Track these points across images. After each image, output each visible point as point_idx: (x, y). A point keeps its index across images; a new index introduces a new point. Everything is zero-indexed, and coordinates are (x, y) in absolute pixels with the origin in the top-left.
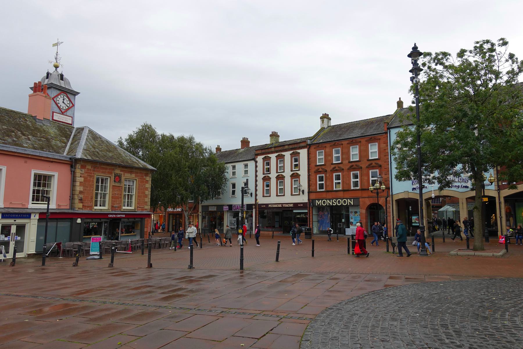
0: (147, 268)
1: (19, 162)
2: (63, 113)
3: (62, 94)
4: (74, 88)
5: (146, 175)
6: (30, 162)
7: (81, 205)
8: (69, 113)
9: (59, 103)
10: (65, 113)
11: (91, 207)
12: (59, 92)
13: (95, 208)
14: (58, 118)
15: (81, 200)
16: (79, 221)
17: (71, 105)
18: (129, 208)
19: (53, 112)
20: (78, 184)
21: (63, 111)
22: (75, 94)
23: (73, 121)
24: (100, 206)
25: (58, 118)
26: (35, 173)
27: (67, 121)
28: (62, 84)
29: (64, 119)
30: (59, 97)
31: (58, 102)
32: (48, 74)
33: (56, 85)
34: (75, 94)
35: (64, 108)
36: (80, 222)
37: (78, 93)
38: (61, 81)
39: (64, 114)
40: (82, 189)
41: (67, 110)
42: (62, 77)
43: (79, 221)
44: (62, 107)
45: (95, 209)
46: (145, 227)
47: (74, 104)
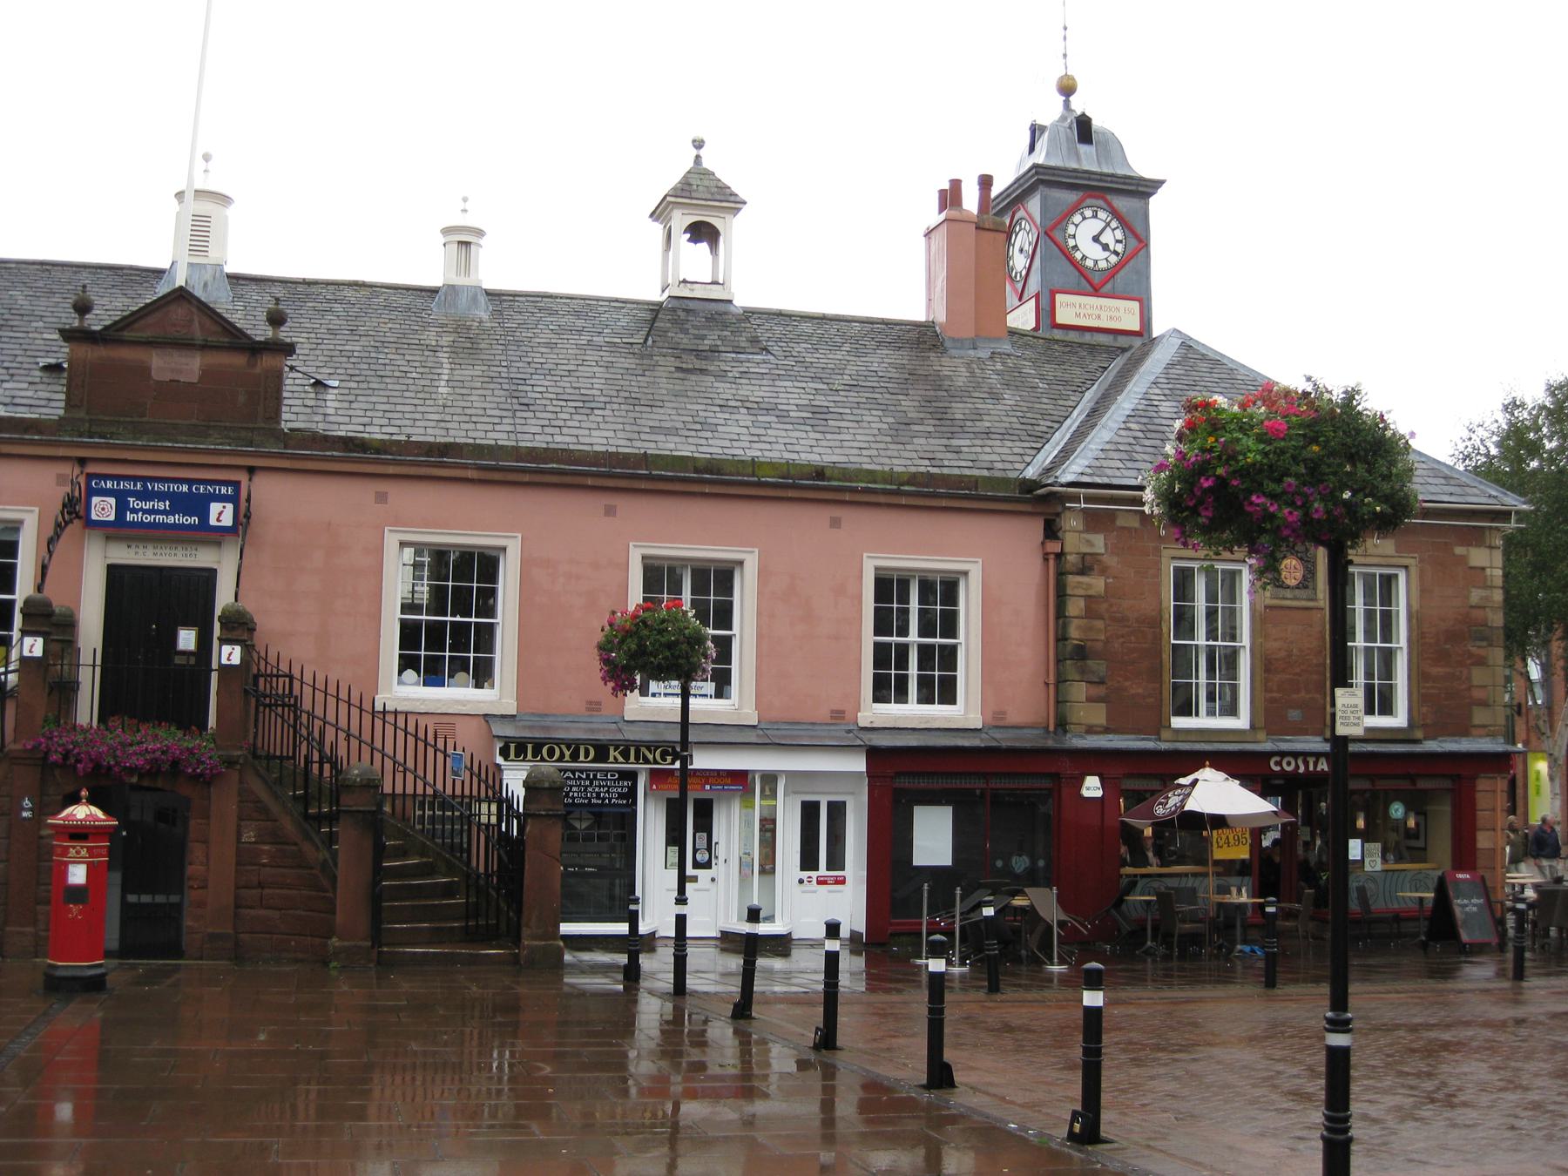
0: (923, 1087)
2: (1096, 291)
3: (1089, 201)
4: (1141, 165)
5: (1475, 537)
6: (859, 522)
7: (1098, 715)
9: (1076, 247)
10: (1108, 286)
11: (1158, 726)
12: (1071, 197)
13: (1178, 722)
14: (1078, 315)
16: (1092, 787)
17: (1133, 243)
18: (938, 713)
20: (1075, 607)
21: (1096, 279)
22: (1143, 189)
24: (1211, 713)
25: (1078, 315)
26: (877, 569)
27: (1119, 319)
28: (1087, 160)
29: (1104, 315)
30: (1077, 218)
31: (1071, 243)
33: (1075, 171)
34: (1143, 189)
35: (1103, 265)
36: (1099, 794)
37: (1157, 184)
38: (1083, 149)
39: (1104, 290)
41: (1114, 271)
42: (1084, 129)
43: (1092, 787)
44: (1090, 263)
45: (1178, 731)
46: (1480, 823)
47: (1143, 236)
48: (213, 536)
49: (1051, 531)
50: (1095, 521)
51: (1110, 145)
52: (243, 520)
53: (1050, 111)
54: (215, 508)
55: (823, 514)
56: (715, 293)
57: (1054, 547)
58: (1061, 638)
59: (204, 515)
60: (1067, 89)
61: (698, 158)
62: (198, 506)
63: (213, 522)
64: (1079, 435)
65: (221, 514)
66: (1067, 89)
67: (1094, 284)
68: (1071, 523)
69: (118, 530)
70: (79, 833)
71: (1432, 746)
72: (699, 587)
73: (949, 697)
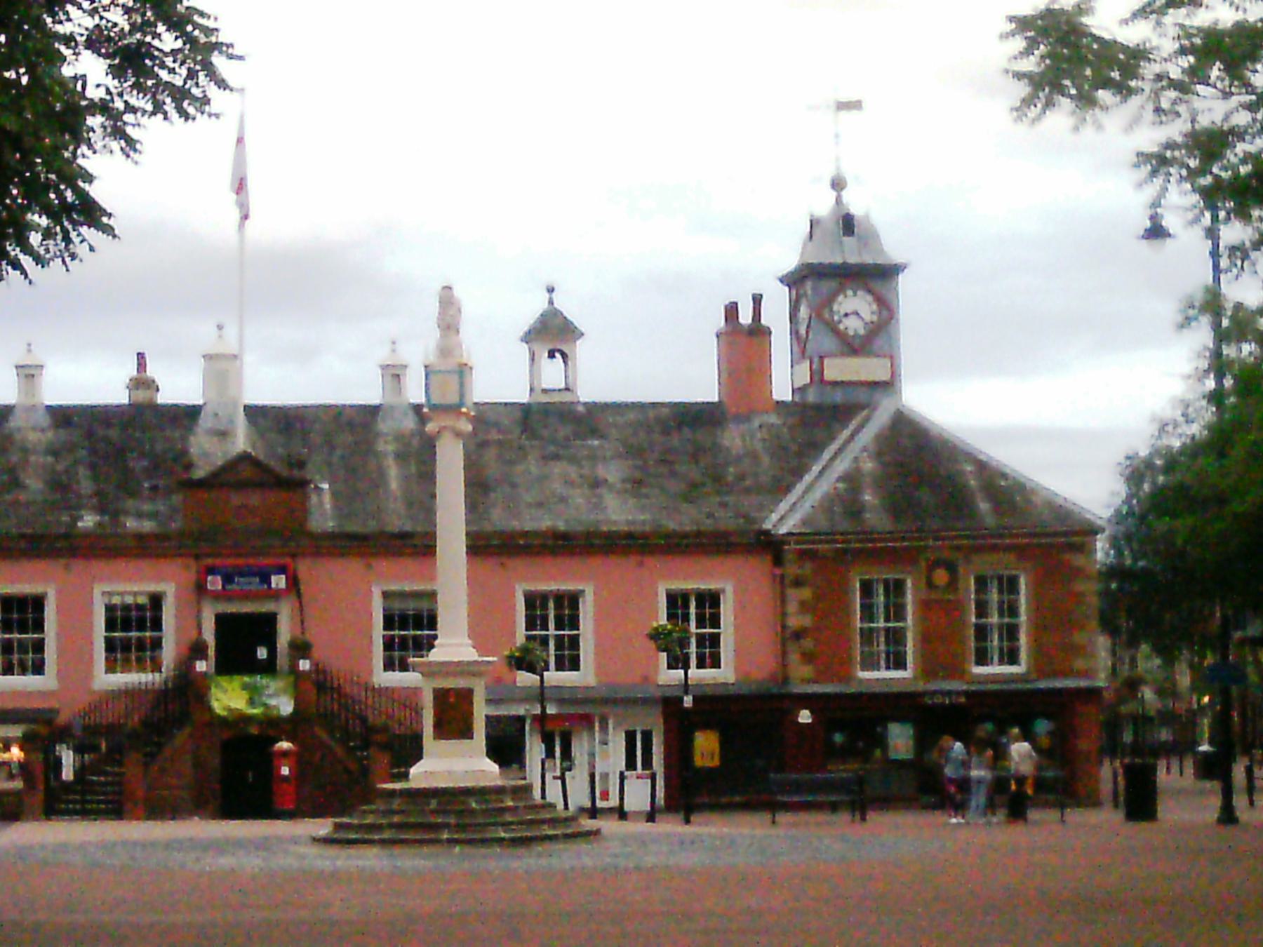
1: (621, 569)
7: (807, 671)
8: (880, 342)
12: (831, 284)
15: (808, 658)
16: (805, 717)
19: (821, 358)
20: (792, 608)
21: (857, 343)
23: (894, 374)
24: (888, 668)
30: (841, 298)
32: (813, 223)
40: (806, 621)
42: (848, 224)
43: (805, 717)
45: (861, 681)
48: (276, 595)
49: (778, 561)
50: (802, 554)
51: (870, 238)
52: (293, 583)
53: (824, 205)
54: (274, 579)
55: (633, 560)
56: (567, 397)
57: (778, 571)
58: (784, 627)
59: (270, 584)
60: (838, 184)
61: (551, 302)
62: (266, 579)
63: (273, 585)
64: (806, 491)
65: (279, 581)
66: (838, 184)
67: (854, 347)
68: (789, 557)
69: (223, 596)
70: (285, 754)
71: (1042, 685)
72: (559, 606)
73: (716, 664)
